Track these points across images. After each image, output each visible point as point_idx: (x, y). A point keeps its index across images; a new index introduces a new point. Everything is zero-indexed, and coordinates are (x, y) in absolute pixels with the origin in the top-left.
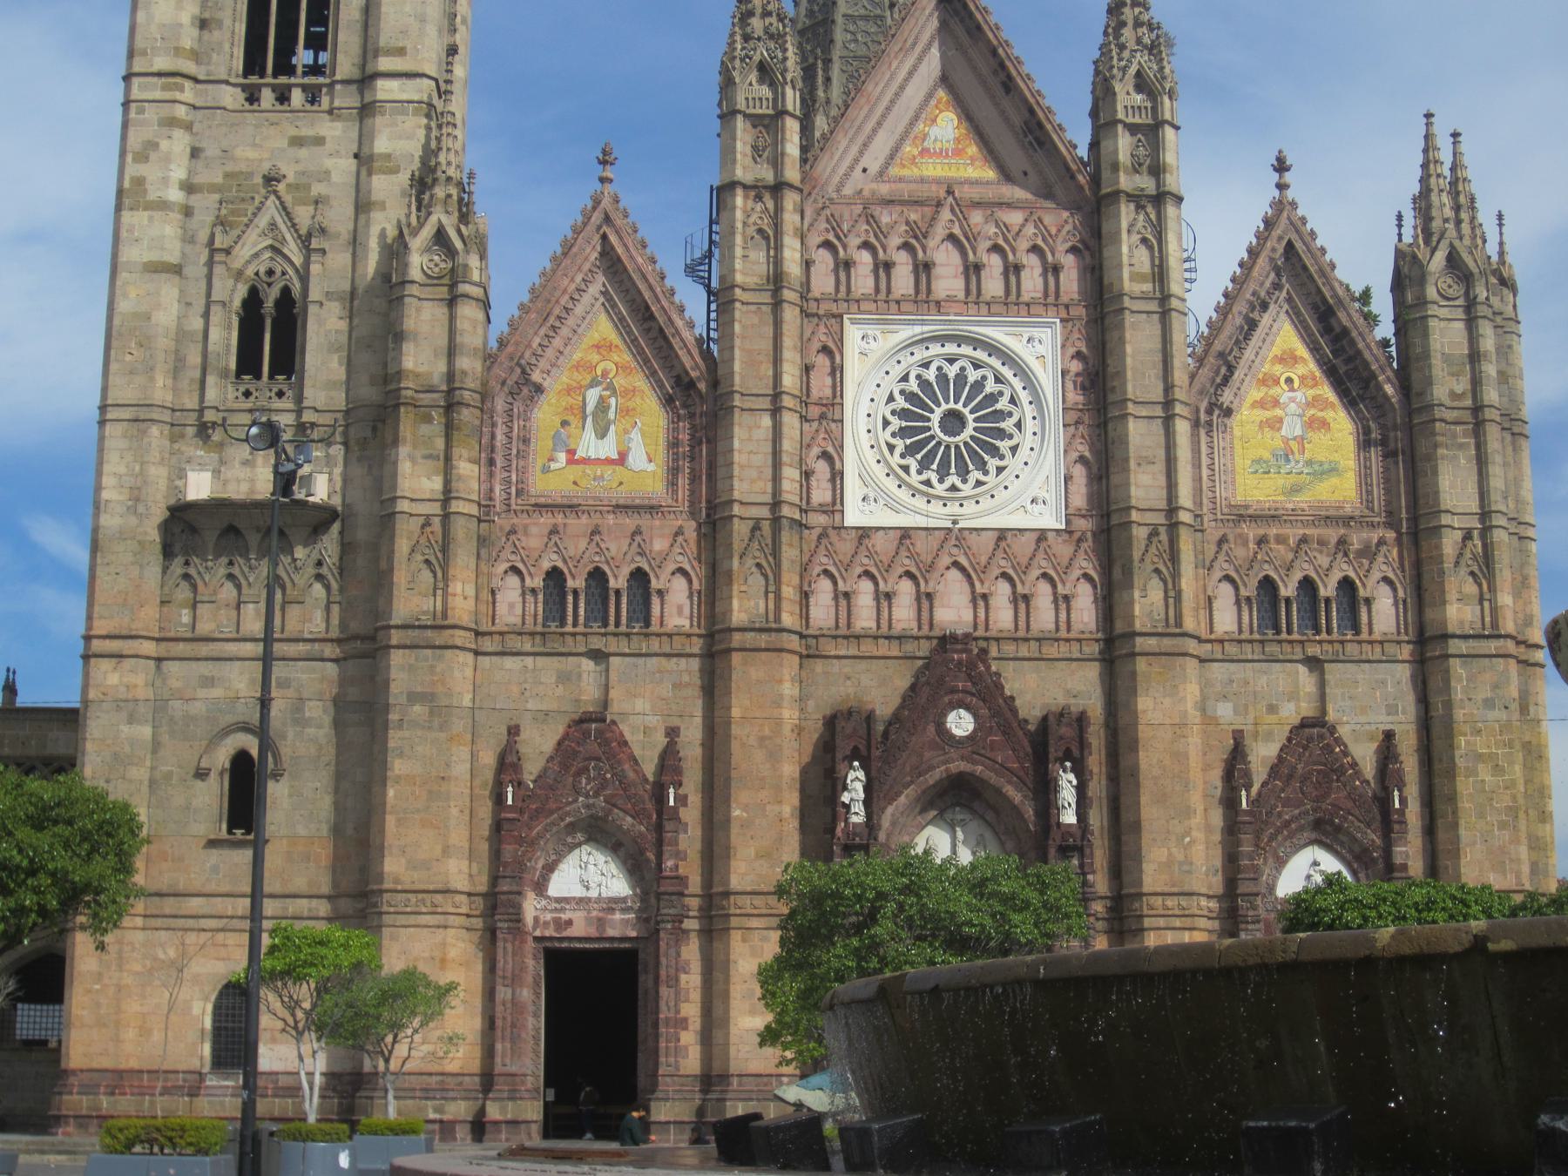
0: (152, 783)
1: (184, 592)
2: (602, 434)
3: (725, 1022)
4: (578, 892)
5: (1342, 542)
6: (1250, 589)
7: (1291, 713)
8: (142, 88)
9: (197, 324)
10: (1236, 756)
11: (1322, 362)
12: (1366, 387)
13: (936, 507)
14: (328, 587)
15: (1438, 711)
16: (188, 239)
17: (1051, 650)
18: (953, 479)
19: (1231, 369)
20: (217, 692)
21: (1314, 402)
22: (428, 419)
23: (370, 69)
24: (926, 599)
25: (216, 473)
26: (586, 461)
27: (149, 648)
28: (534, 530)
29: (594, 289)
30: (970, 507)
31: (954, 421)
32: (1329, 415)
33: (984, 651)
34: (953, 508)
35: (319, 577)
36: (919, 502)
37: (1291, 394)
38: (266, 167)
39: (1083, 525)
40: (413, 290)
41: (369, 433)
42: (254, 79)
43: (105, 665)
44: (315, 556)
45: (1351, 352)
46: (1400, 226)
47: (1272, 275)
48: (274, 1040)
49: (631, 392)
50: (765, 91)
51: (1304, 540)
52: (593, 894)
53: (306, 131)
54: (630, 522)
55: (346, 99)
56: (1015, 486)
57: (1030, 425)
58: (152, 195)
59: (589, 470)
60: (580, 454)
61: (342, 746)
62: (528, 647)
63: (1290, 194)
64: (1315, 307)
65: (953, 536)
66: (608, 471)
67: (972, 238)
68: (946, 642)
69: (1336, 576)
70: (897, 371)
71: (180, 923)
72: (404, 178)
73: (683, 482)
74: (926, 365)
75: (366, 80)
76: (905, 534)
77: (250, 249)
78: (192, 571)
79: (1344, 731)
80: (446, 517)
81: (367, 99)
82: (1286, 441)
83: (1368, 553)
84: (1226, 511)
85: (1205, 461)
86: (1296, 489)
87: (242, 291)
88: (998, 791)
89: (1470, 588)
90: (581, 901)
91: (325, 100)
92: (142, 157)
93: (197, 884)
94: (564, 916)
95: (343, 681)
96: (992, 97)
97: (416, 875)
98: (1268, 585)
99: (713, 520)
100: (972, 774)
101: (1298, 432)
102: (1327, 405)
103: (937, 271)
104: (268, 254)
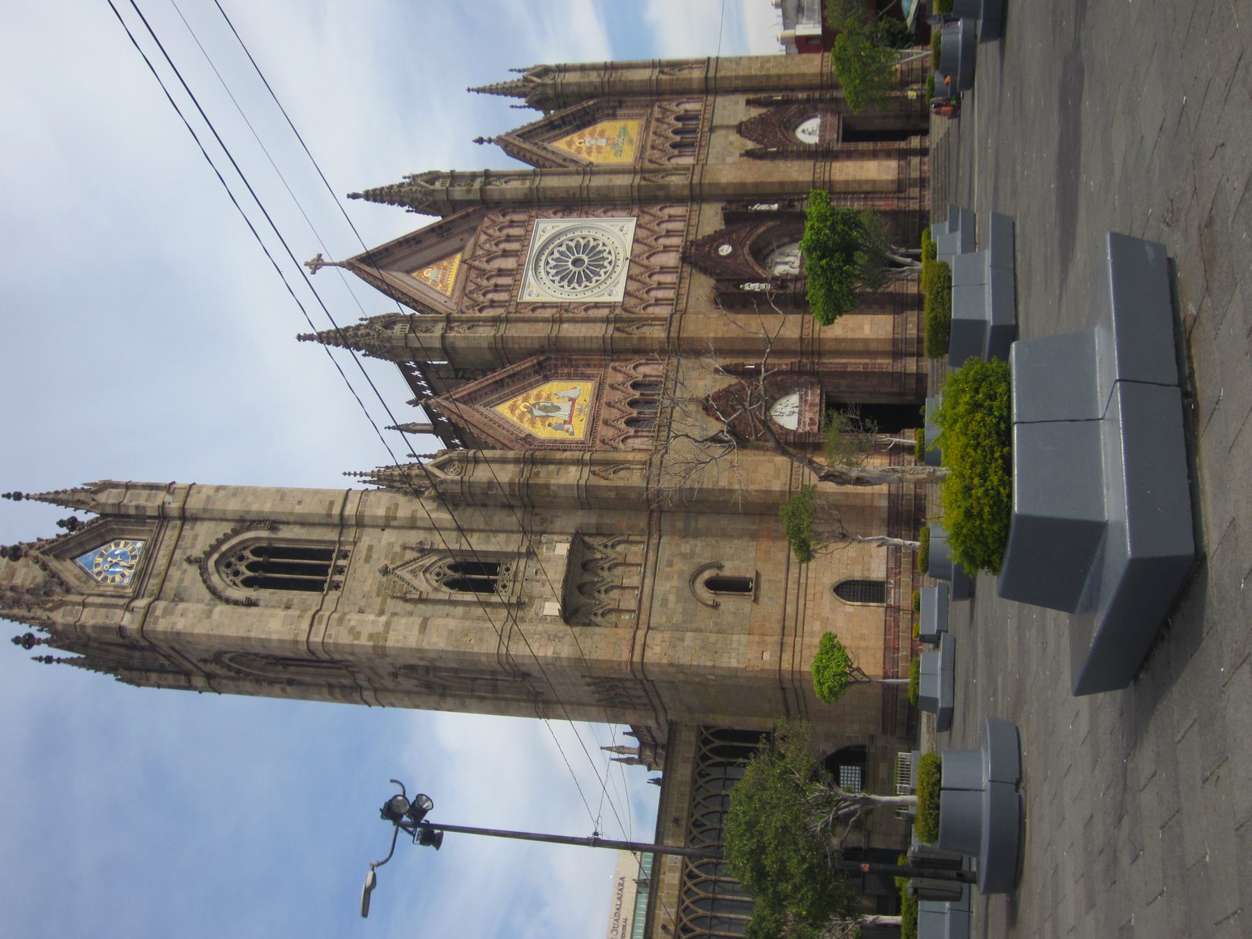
0: (718, 632)
1: (613, 617)
2: (558, 409)
3: (866, 341)
4: (795, 417)
5: (658, 120)
6: (676, 152)
7: (734, 137)
8: (317, 635)
9: (460, 610)
10: (749, 154)
11: (574, 132)
12: (587, 113)
13: (618, 270)
14: (620, 543)
15: (739, 83)
16: (411, 614)
17: (694, 222)
18: (606, 263)
20: (672, 598)
21: (592, 135)
22: (537, 474)
23: (336, 520)
24: (663, 270)
25: (546, 600)
26: (571, 416)
27: (641, 633)
28: (604, 433)
29: (482, 409)
30: (621, 256)
31: (576, 262)
33: (692, 242)
34: (620, 263)
35: (613, 546)
36: (614, 276)
38: (379, 575)
39: (636, 211)
40: (466, 479)
41: (538, 518)
42: (326, 586)
43: (648, 654)
44: (601, 548)
48: (869, 570)
49: (538, 397)
50: (398, 327)
51: (655, 133)
52: (797, 410)
53: (363, 556)
54: (607, 390)
55: (350, 535)
56: (612, 239)
57: (585, 233)
58: (381, 629)
59: (575, 413)
60: (567, 418)
61: (707, 533)
62: (665, 434)
63: (494, 137)
64: (548, 131)
65: (633, 261)
66: (577, 406)
67: (489, 252)
68: (684, 259)
69: (673, 122)
70: (549, 284)
71: (800, 617)
72: (401, 499)
73: (589, 371)
74: (548, 273)
75: (342, 524)
76: (629, 277)
77: (423, 584)
78: (600, 612)
79: (744, 119)
80: (592, 463)
81: (353, 522)
82: (608, 144)
83: (665, 111)
86: (631, 142)
87: (444, 588)
88: (760, 236)
89: (686, 72)
90: (800, 413)
91: (348, 548)
92: (357, 635)
93: (779, 609)
94: (808, 421)
95: (673, 532)
96: (421, 250)
97: (782, 475)
98: (674, 146)
99: (612, 352)
100: (751, 246)
103: (503, 267)
104: (428, 575)
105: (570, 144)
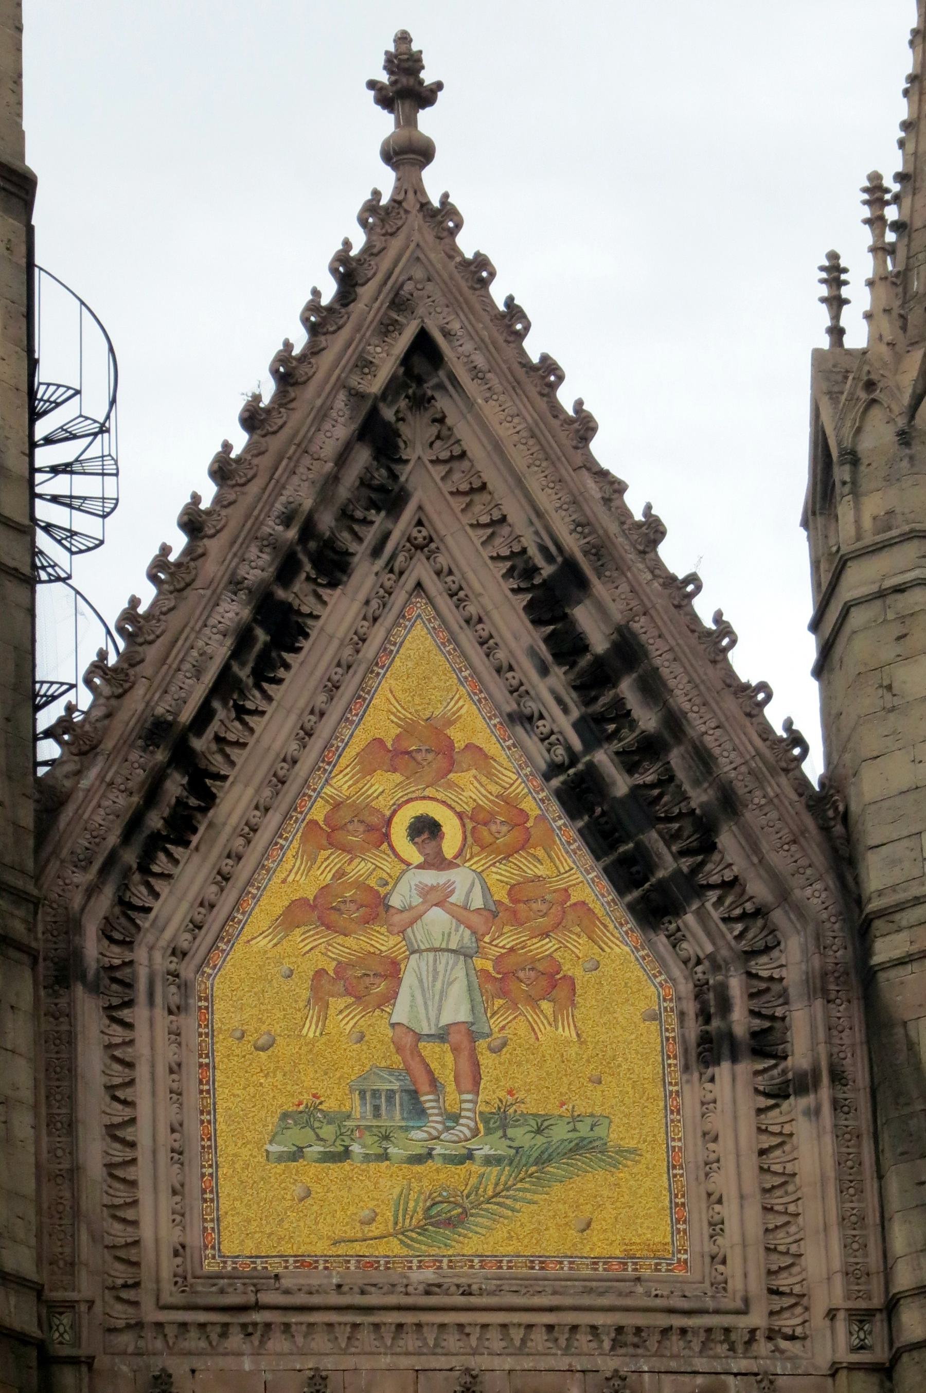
19: (203, 788)
21: (514, 906)
32: (571, 951)
37: (431, 877)
45: (647, 720)
46: (836, 303)
47: (363, 457)
63: (435, 182)
64: (520, 569)
82: (409, 1041)
84: (170, 1295)
85: (94, 1109)
86: (445, 1216)
101: (456, 1011)
102: (566, 914)
105: (425, 751)
